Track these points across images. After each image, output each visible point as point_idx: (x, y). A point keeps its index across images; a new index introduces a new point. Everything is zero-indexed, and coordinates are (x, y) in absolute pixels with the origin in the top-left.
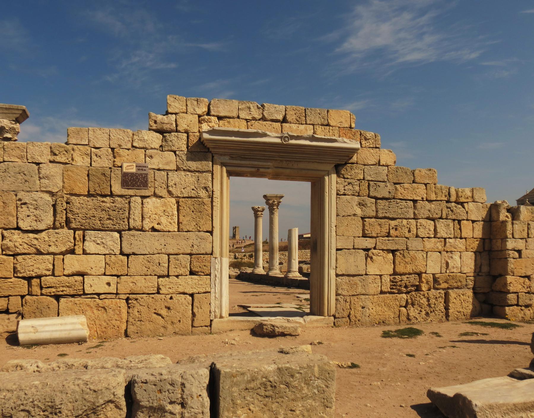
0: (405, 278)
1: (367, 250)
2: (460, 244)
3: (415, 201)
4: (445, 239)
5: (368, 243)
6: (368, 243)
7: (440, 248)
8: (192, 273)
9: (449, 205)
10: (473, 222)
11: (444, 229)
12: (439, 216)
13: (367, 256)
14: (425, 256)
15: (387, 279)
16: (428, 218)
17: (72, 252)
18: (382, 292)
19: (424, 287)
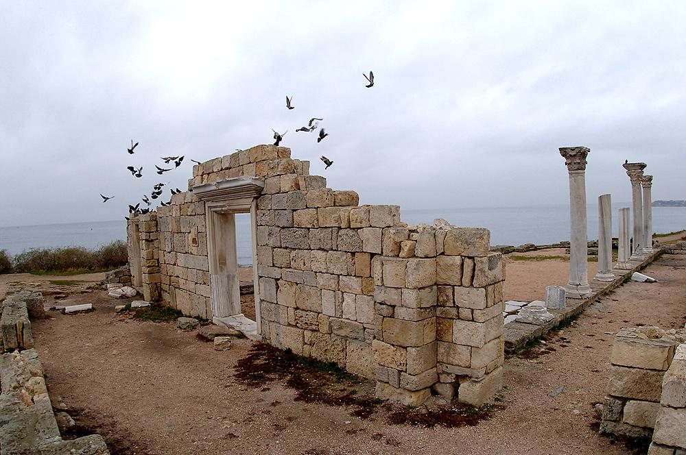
0: (304, 313)
1: (277, 280)
2: (355, 283)
3: (309, 229)
4: (339, 276)
5: (276, 273)
6: (276, 273)
7: (334, 286)
8: (205, 284)
9: (342, 232)
10: (372, 255)
12: (328, 247)
13: (278, 287)
14: (319, 294)
15: (291, 311)
16: (320, 249)
17: (175, 265)
18: (289, 325)
19: (324, 328)
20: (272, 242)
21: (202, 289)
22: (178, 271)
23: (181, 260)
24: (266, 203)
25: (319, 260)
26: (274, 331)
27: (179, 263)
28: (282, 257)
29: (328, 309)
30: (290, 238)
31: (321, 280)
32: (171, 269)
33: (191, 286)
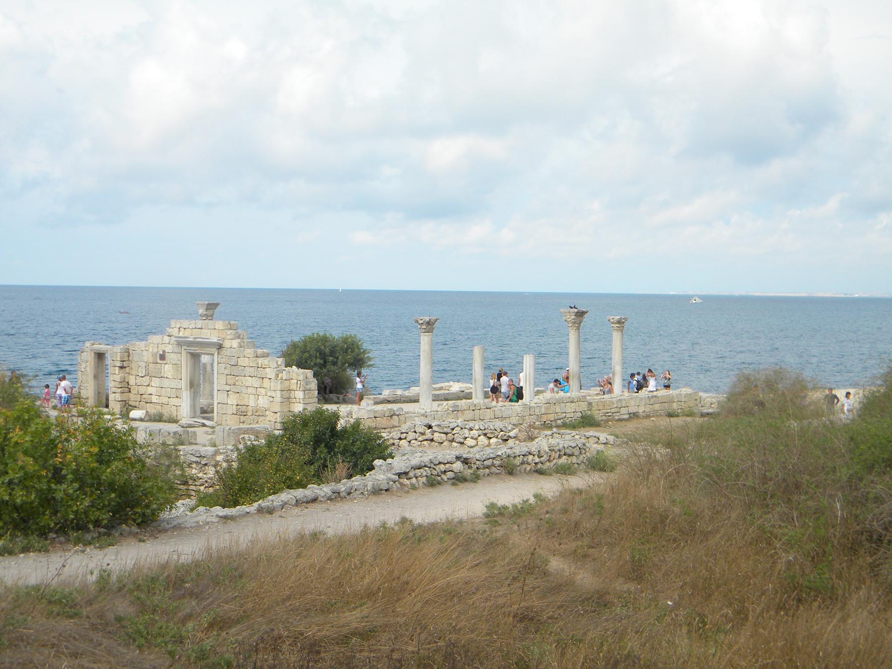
2: (263, 391)
11: (255, 382)
15: (235, 407)
19: (249, 413)
20: (226, 372)
21: (174, 401)
22: (150, 390)
23: (156, 382)
24: (224, 352)
25: (249, 381)
26: (224, 419)
27: (153, 384)
28: (231, 380)
29: (252, 403)
30: (235, 371)
31: (250, 390)
32: (142, 390)
33: (165, 400)
